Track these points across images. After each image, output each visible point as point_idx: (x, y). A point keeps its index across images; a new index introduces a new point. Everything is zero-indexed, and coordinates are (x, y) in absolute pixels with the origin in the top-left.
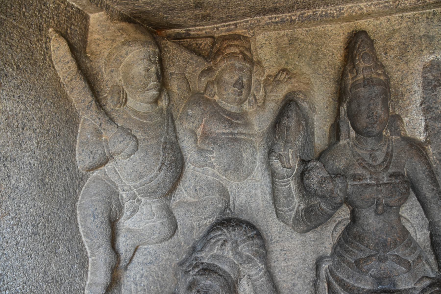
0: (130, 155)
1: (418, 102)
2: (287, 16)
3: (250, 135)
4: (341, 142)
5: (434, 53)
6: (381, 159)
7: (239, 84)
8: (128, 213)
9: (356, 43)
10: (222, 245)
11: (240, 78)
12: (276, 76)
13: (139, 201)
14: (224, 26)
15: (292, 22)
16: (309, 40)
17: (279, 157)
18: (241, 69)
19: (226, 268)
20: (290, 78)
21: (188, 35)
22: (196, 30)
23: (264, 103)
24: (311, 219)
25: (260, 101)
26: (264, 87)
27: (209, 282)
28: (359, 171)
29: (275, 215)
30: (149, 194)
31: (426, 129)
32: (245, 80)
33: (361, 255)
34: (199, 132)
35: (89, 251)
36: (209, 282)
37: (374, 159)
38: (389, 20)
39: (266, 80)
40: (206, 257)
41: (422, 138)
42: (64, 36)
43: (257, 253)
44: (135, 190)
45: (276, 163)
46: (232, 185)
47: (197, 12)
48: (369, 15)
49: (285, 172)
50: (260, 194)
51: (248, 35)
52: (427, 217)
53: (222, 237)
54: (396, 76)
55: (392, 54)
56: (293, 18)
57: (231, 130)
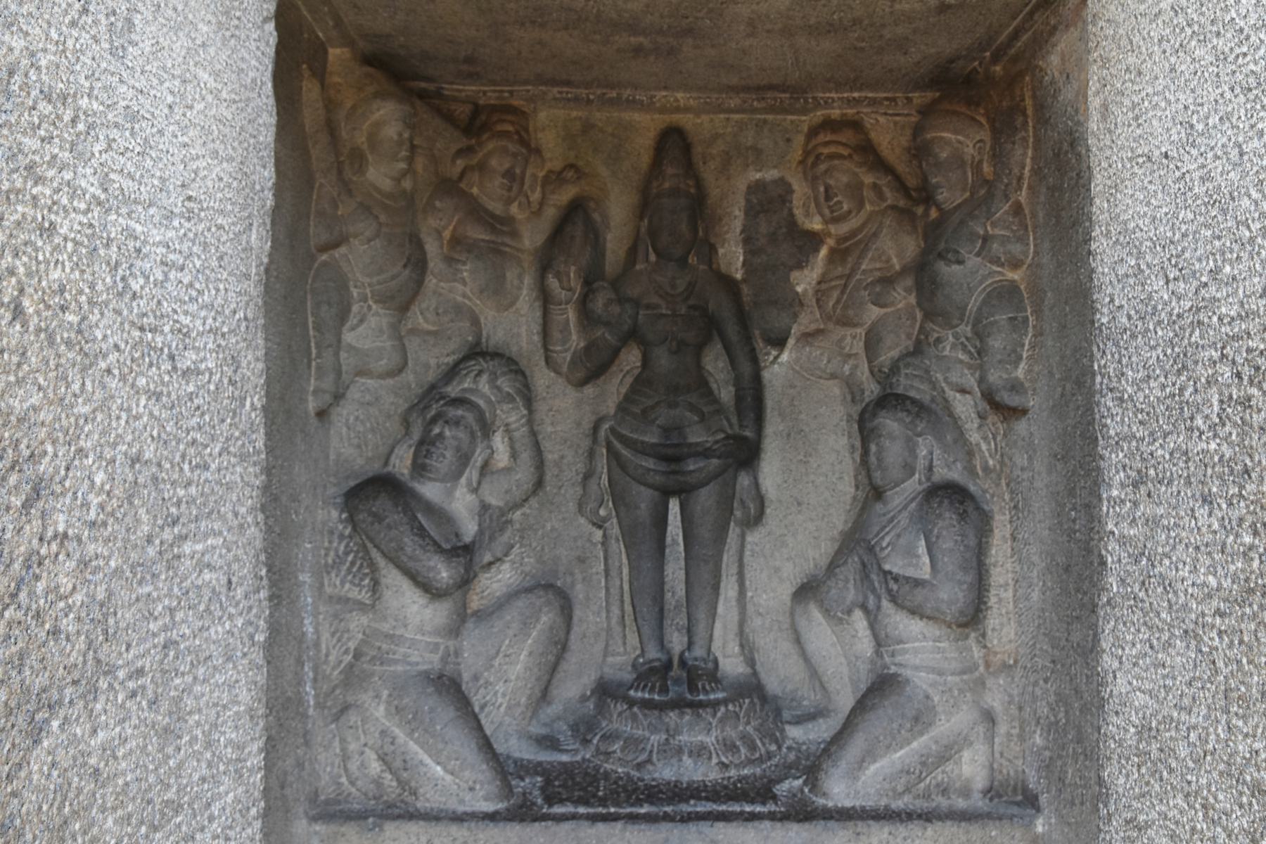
0: (369, 240)
1: (738, 230)
2: (583, 92)
3: (518, 250)
4: (638, 267)
5: (760, 171)
6: (680, 290)
7: (509, 174)
8: (355, 321)
9: (673, 143)
10: (477, 376)
11: (512, 167)
12: (560, 173)
13: (370, 308)
14: (495, 91)
15: (589, 102)
16: (610, 130)
17: (558, 275)
18: (515, 155)
19: (481, 403)
20: (578, 178)
21: (438, 94)
22: (453, 90)
23: (540, 209)
24: (592, 368)
25: (535, 206)
26: (543, 187)
27: (460, 412)
28: (655, 300)
29: (543, 363)
30: (382, 299)
31: (744, 264)
32: (518, 171)
33: (650, 403)
34: (447, 234)
35: (314, 351)
36: (460, 412)
37: (673, 286)
38: (712, 120)
39: (546, 177)
40: (453, 390)
41: (739, 276)
42: (314, 73)
43: (519, 392)
44: (368, 291)
45: (553, 282)
46: (488, 315)
47: (465, 67)
48: (687, 110)
49: (564, 295)
50: (524, 334)
51: (525, 109)
52: (734, 369)
53: (477, 367)
54: (714, 193)
55: (712, 165)
56: (591, 97)
57: (493, 238)
